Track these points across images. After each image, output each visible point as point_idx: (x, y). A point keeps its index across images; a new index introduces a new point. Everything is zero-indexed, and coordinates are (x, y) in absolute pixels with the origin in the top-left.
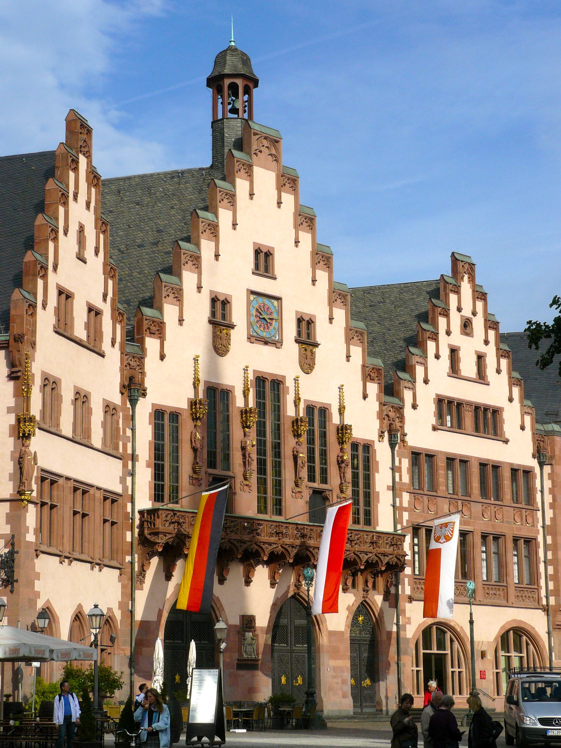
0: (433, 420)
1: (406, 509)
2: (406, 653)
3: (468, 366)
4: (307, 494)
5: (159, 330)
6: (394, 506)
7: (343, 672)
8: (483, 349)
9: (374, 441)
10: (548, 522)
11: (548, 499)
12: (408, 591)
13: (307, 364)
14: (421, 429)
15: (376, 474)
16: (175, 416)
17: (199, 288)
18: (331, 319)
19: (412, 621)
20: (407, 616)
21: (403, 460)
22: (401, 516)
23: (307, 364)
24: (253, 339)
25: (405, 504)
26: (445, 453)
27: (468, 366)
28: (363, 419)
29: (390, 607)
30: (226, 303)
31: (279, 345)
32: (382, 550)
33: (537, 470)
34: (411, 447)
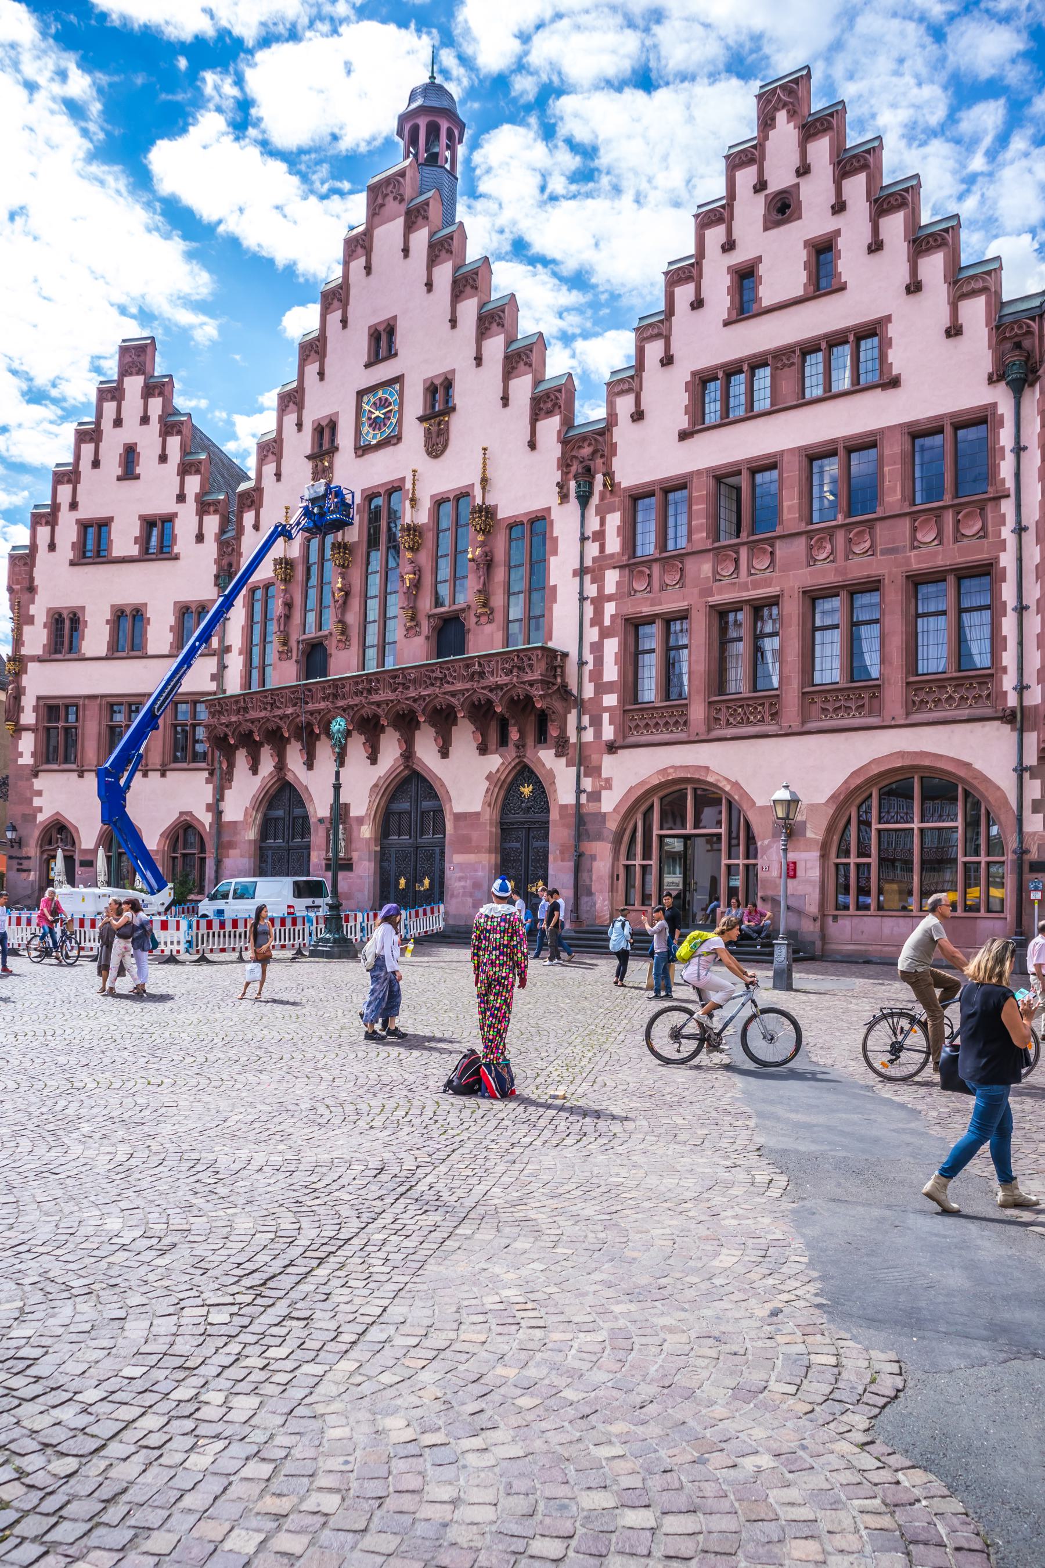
0: (684, 423)
1: (610, 598)
2: (599, 837)
4: (425, 627)
6: (582, 599)
7: (476, 871)
9: (549, 509)
10: (1032, 514)
11: (1033, 459)
12: (608, 733)
13: (436, 444)
15: (552, 559)
17: (299, 425)
19: (614, 783)
20: (604, 775)
21: (609, 517)
22: (599, 613)
23: (436, 444)
24: (360, 452)
25: (610, 588)
26: (708, 470)
28: (526, 483)
29: (568, 766)
30: (333, 425)
32: (492, 680)
33: (1005, 408)
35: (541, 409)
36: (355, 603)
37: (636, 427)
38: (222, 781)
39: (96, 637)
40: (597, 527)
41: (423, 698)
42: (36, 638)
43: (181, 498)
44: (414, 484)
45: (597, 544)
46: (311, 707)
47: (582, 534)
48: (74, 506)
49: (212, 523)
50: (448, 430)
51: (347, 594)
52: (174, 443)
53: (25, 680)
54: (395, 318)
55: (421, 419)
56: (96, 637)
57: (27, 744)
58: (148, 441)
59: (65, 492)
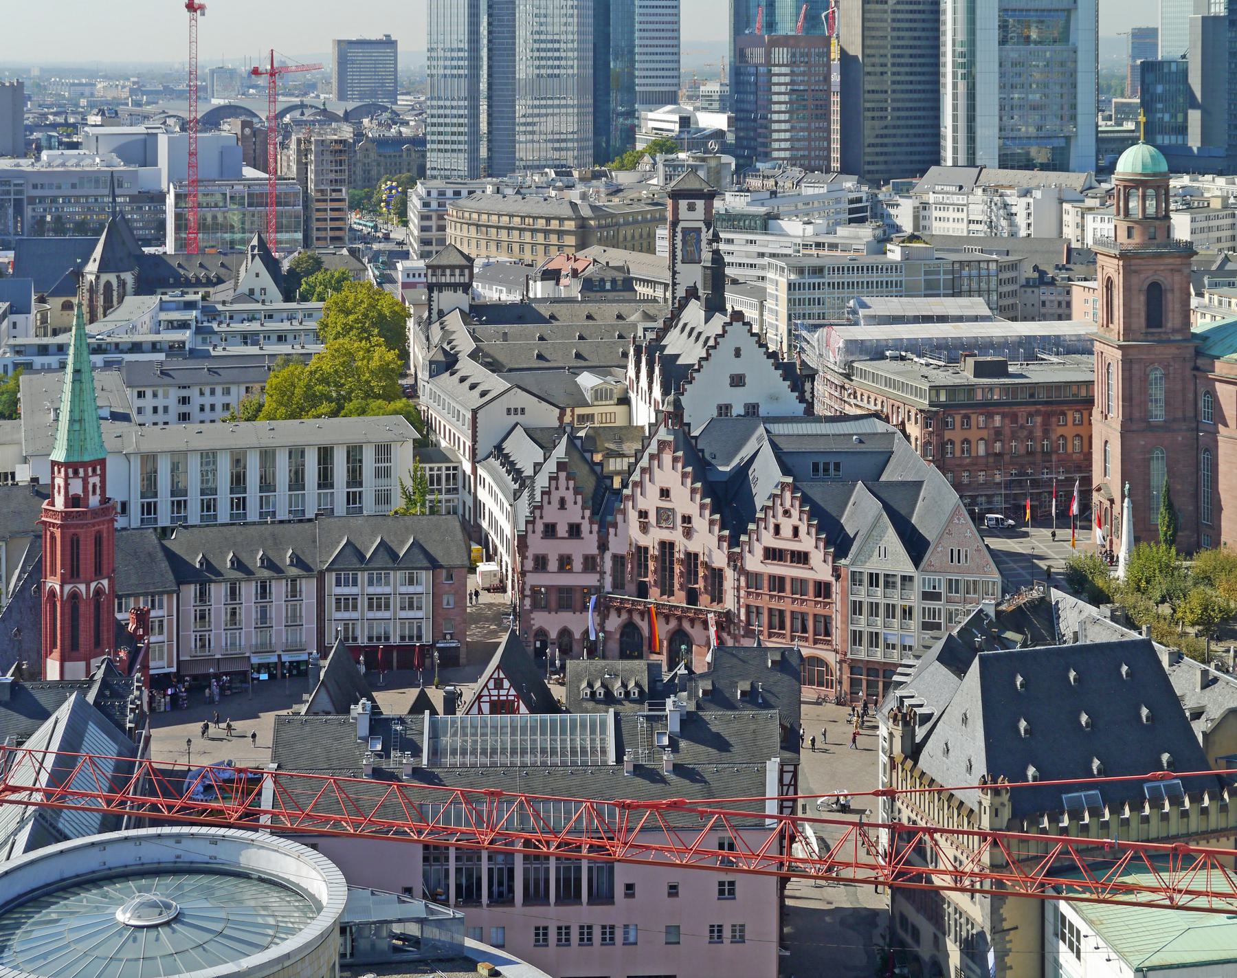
3: (786, 531)
5: (615, 525)
8: (797, 523)
13: (688, 533)
14: (754, 562)
16: (622, 557)
23: (688, 533)
27: (786, 531)
38: (604, 617)
39: (553, 565)
42: (529, 564)
43: (583, 518)
48: (541, 517)
49: (595, 527)
52: (579, 498)
53: (526, 579)
56: (553, 565)
57: (528, 602)
58: (569, 496)
59: (537, 513)
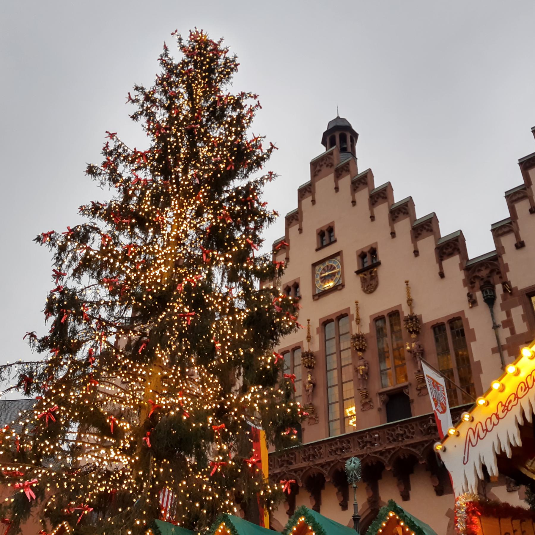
4: (378, 402)
9: (463, 312)
15: (472, 344)
18: (393, 234)
24: (316, 297)
30: (296, 286)
31: (340, 287)
34: (522, 291)
35: (444, 253)
36: (320, 391)
37: (520, 252)
40: (505, 318)
41: (388, 451)
44: (357, 309)
45: (507, 330)
46: (295, 466)
47: (494, 323)
50: (377, 276)
51: (314, 385)
54: (333, 222)
55: (358, 272)
